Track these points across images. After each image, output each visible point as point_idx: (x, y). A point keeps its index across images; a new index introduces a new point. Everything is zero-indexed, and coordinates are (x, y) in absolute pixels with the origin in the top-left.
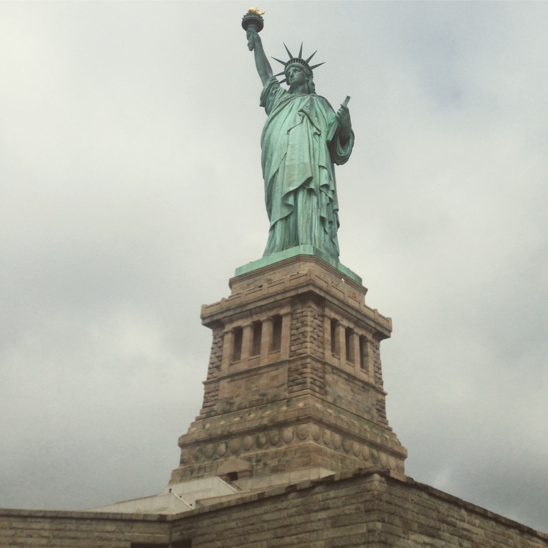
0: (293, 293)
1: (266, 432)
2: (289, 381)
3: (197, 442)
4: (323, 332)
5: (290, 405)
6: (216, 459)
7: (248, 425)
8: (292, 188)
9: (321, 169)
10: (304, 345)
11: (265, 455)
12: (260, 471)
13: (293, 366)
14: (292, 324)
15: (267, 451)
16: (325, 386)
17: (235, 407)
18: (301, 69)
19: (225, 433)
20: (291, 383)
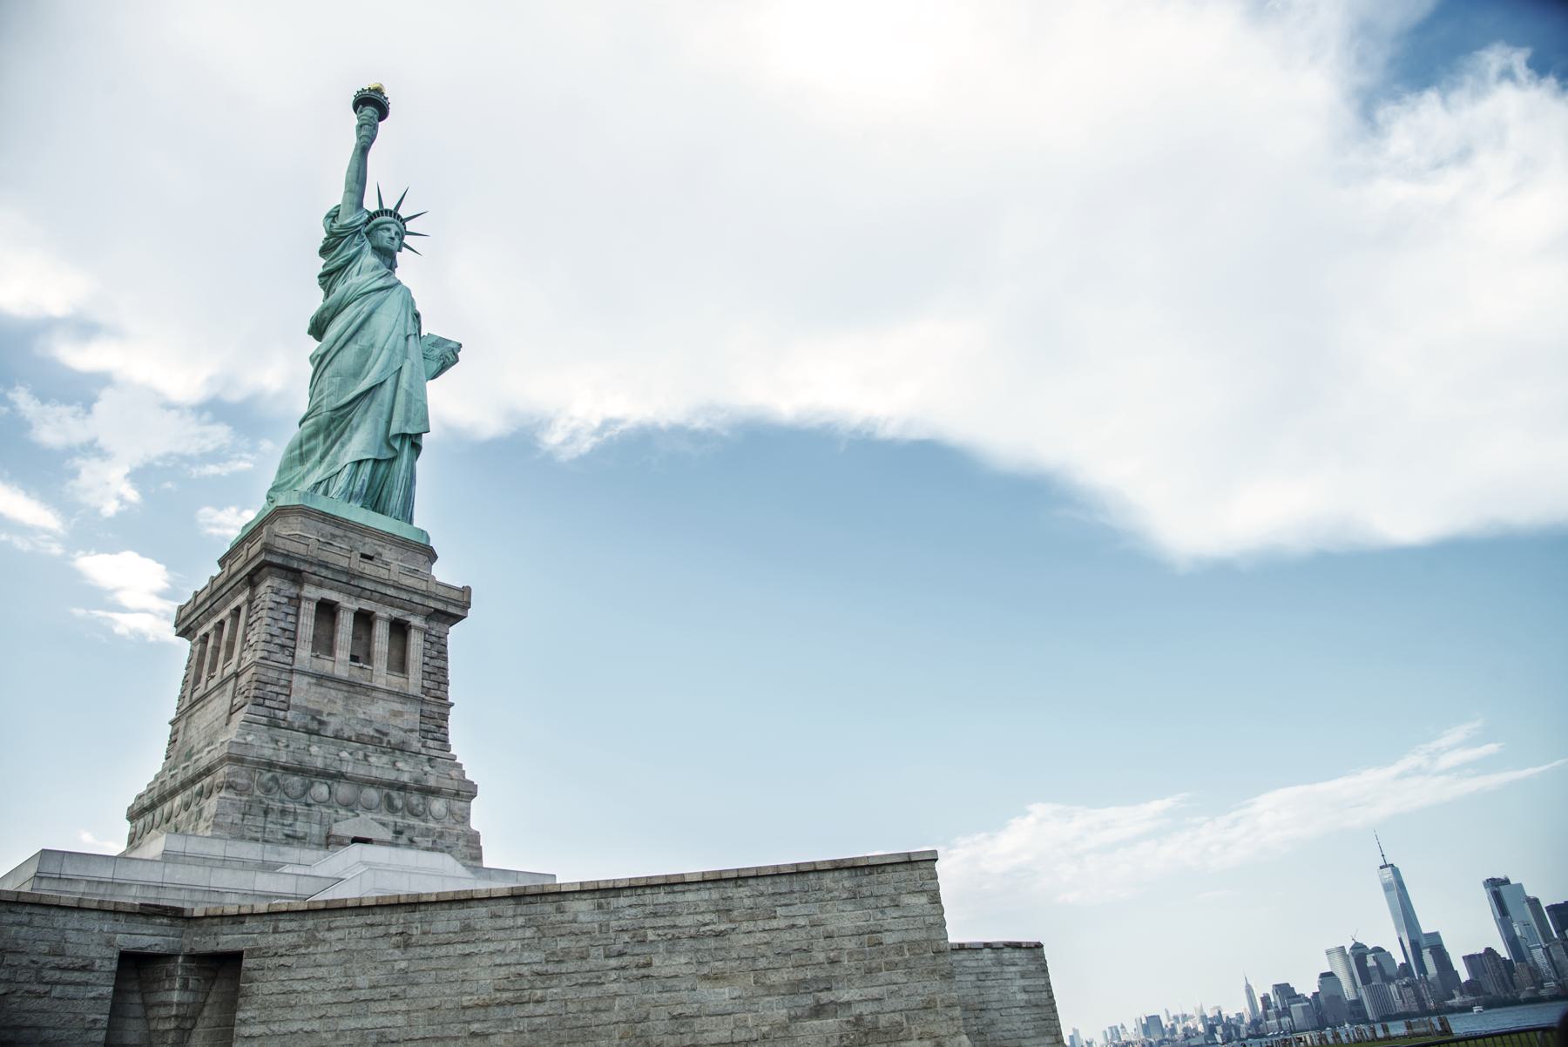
0: (440, 606)
1: (402, 793)
2: (421, 730)
3: (271, 765)
7: (375, 773)
8: (409, 432)
10: (443, 687)
11: (410, 827)
13: (425, 707)
19: (332, 771)
20: (423, 732)
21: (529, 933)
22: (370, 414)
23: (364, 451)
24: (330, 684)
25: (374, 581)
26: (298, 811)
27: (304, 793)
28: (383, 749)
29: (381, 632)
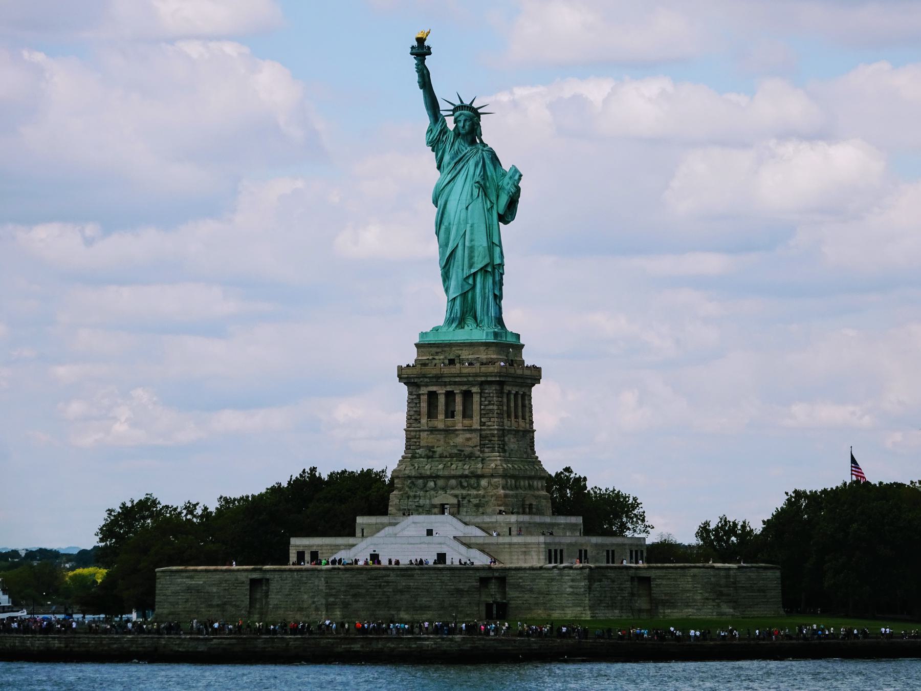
0: (483, 379)
1: (467, 479)
3: (409, 477)
4: (502, 405)
5: (484, 463)
6: (427, 491)
7: (453, 473)
8: (473, 271)
9: (494, 245)
10: (492, 420)
11: (469, 495)
12: (465, 505)
14: (481, 401)
15: (469, 492)
16: (504, 446)
17: (437, 456)
18: (471, 119)
21: (291, 579)
22: (454, 268)
23: (454, 293)
24: (437, 433)
25: (449, 377)
26: (421, 495)
27: (425, 485)
28: (460, 459)
29: (459, 399)
